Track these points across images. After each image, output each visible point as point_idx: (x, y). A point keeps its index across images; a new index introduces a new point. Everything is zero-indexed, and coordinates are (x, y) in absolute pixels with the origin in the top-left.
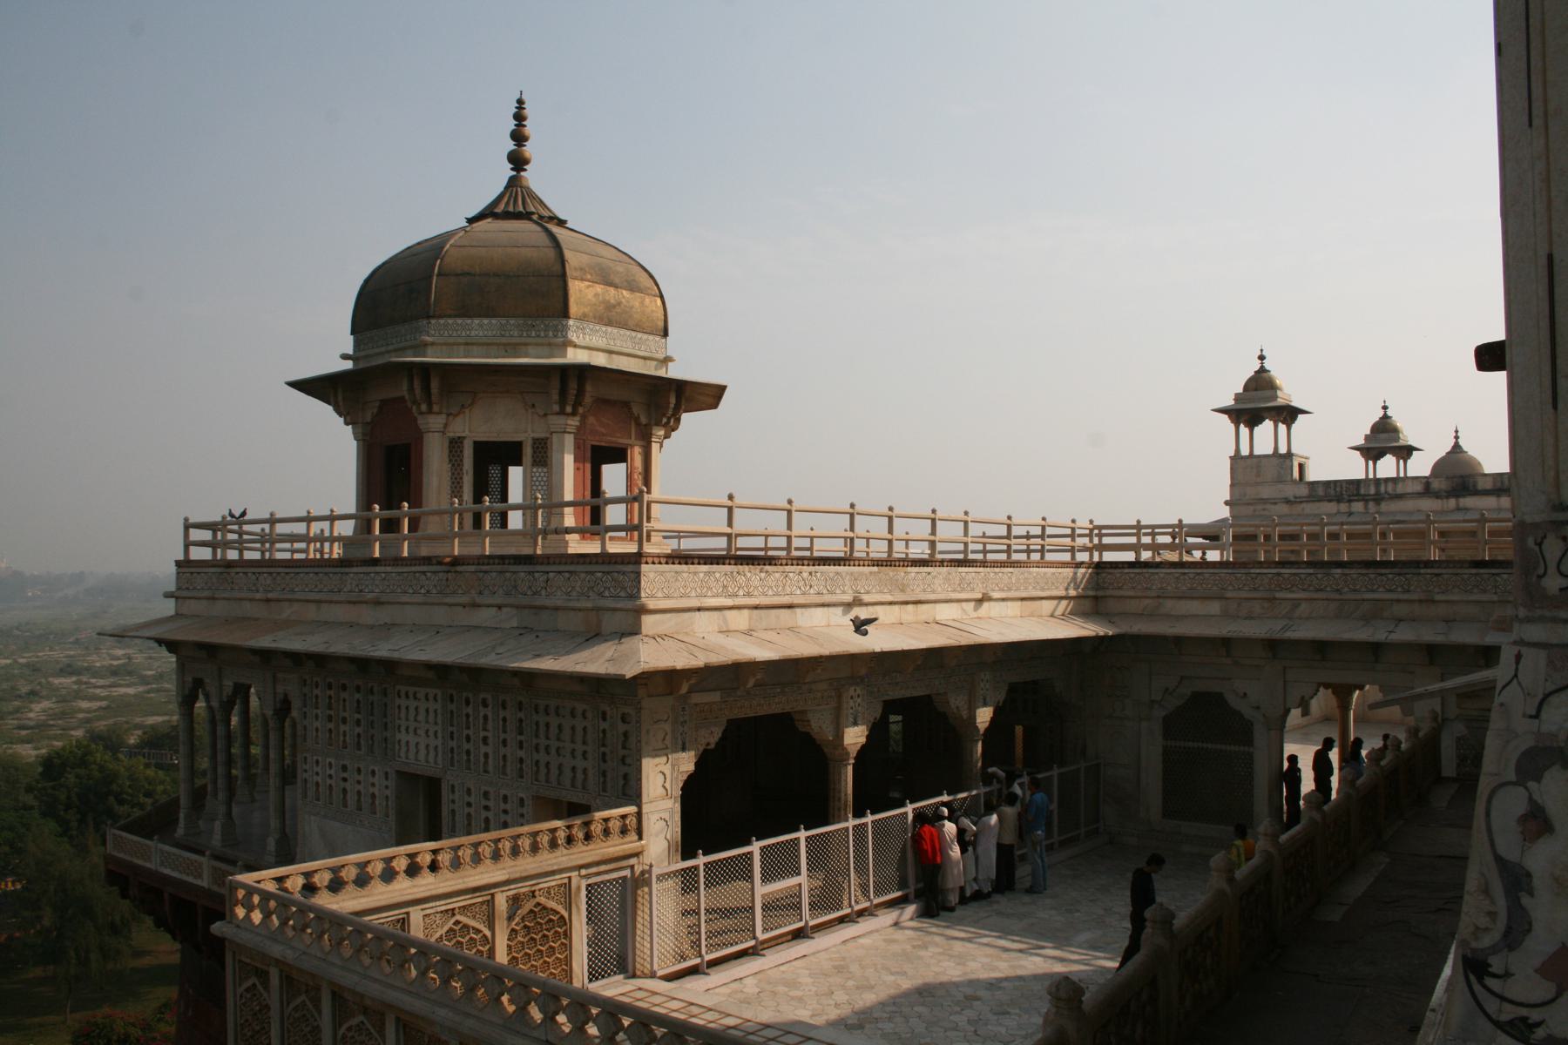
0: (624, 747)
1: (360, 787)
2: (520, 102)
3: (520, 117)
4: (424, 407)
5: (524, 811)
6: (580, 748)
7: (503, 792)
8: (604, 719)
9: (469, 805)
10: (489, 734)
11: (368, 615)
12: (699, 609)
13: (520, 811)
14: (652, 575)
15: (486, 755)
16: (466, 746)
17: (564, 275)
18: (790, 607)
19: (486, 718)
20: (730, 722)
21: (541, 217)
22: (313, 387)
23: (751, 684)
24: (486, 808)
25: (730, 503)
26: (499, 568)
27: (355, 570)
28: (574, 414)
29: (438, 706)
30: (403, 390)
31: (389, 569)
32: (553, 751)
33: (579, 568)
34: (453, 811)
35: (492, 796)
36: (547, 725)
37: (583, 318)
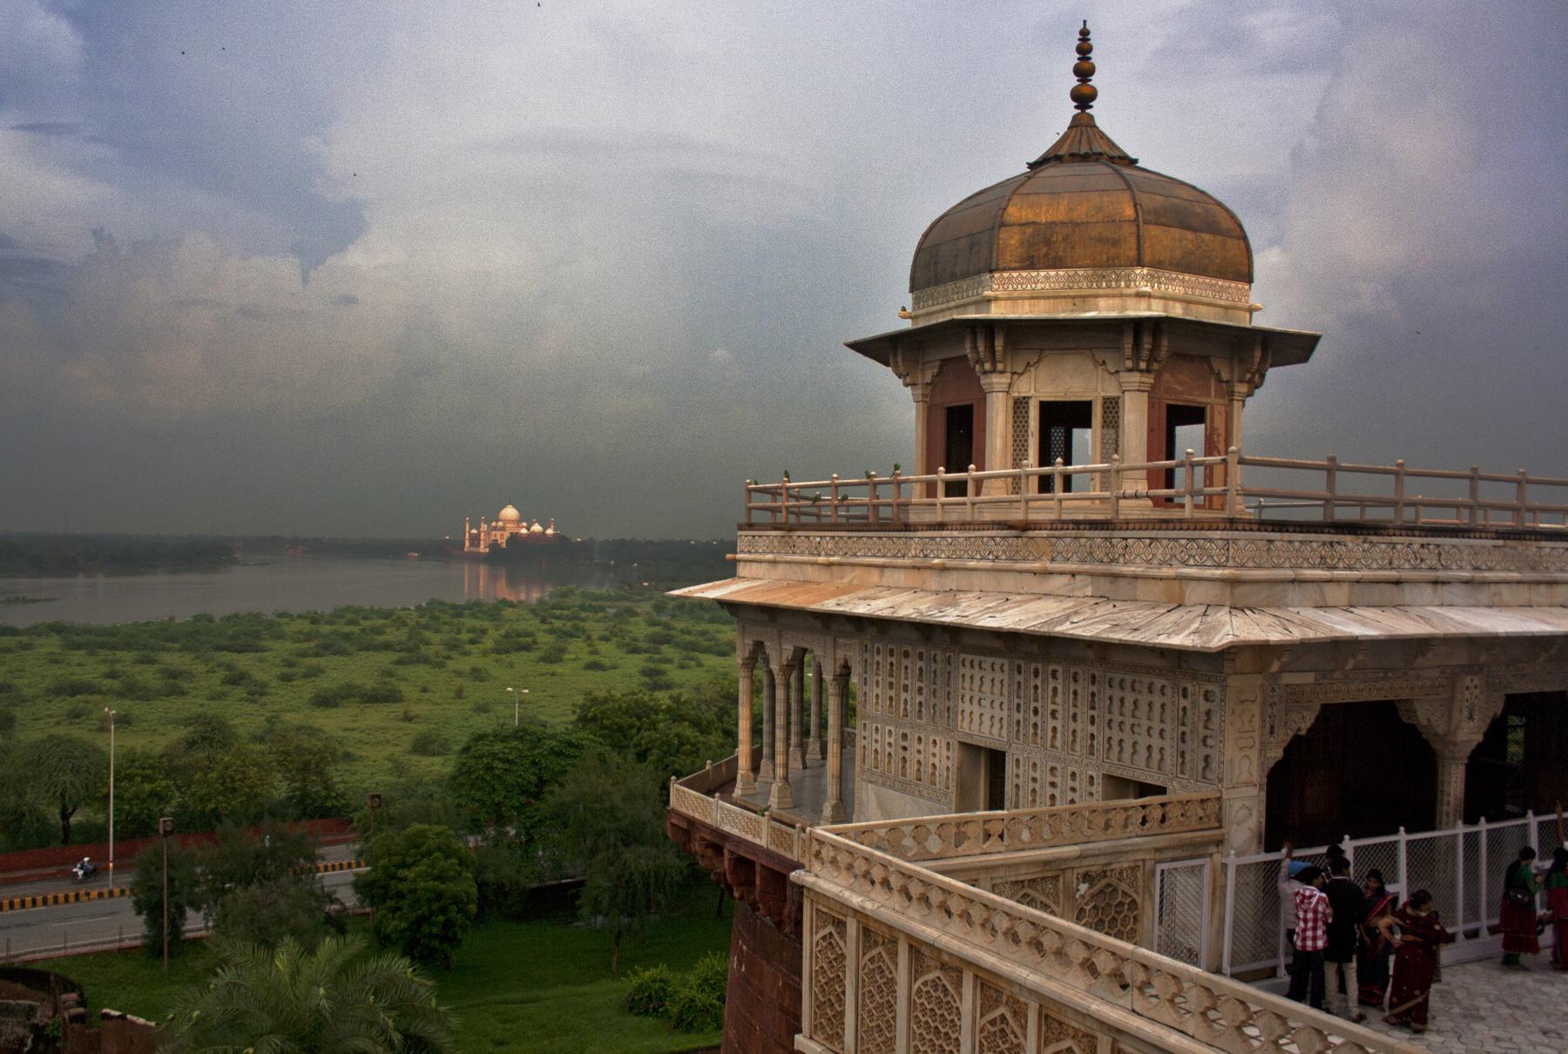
0: (1206, 727)
2: (1084, 34)
3: (1084, 50)
4: (987, 366)
5: (1094, 789)
7: (1070, 769)
8: (1185, 696)
9: (1034, 780)
10: (1059, 708)
12: (1293, 581)
15: (1054, 729)
17: (1136, 220)
18: (1397, 582)
19: (1055, 690)
20: (1324, 706)
21: (1111, 158)
22: (879, 348)
23: (1351, 664)
26: (1073, 533)
27: (919, 534)
28: (1148, 371)
29: (1006, 677)
30: (968, 350)
31: (955, 533)
32: (1127, 728)
33: (1161, 534)
35: (1059, 773)
36: (1122, 700)
37: (1157, 265)
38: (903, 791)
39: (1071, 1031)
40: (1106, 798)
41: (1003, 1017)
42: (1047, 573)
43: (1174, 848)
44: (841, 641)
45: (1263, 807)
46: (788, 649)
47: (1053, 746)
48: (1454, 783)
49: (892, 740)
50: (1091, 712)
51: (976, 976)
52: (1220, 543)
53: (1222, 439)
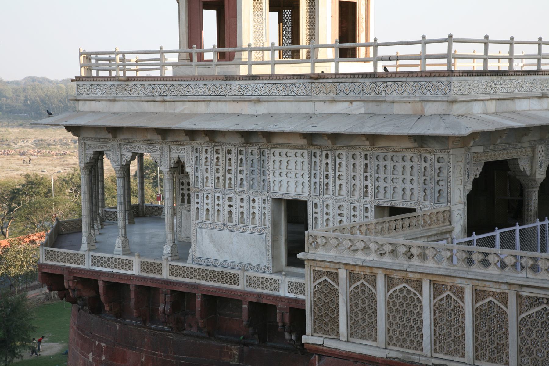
0: (438, 176)
1: (244, 210)
5: (369, 214)
6: (408, 178)
7: (353, 205)
8: (425, 161)
9: (327, 214)
11: (248, 109)
12: (475, 100)
13: (366, 214)
14: (456, 82)
16: (326, 181)
18: (512, 99)
19: (340, 164)
24: (340, 215)
25: (486, 41)
26: (351, 80)
27: (237, 82)
29: (306, 160)
31: (265, 82)
33: (408, 79)
34: (316, 218)
36: (385, 166)
38: (231, 231)
39: (491, 294)
40: (376, 218)
41: (448, 296)
42: (334, 101)
43: (434, 235)
44: (174, 147)
45: (466, 214)
46: (127, 154)
47: (339, 195)
48: (533, 200)
49: (220, 202)
50: (365, 174)
51: (430, 280)
52: (446, 83)
53: (364, 20)
